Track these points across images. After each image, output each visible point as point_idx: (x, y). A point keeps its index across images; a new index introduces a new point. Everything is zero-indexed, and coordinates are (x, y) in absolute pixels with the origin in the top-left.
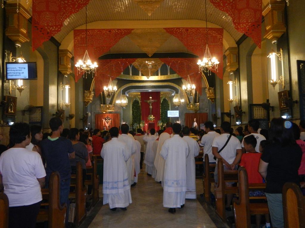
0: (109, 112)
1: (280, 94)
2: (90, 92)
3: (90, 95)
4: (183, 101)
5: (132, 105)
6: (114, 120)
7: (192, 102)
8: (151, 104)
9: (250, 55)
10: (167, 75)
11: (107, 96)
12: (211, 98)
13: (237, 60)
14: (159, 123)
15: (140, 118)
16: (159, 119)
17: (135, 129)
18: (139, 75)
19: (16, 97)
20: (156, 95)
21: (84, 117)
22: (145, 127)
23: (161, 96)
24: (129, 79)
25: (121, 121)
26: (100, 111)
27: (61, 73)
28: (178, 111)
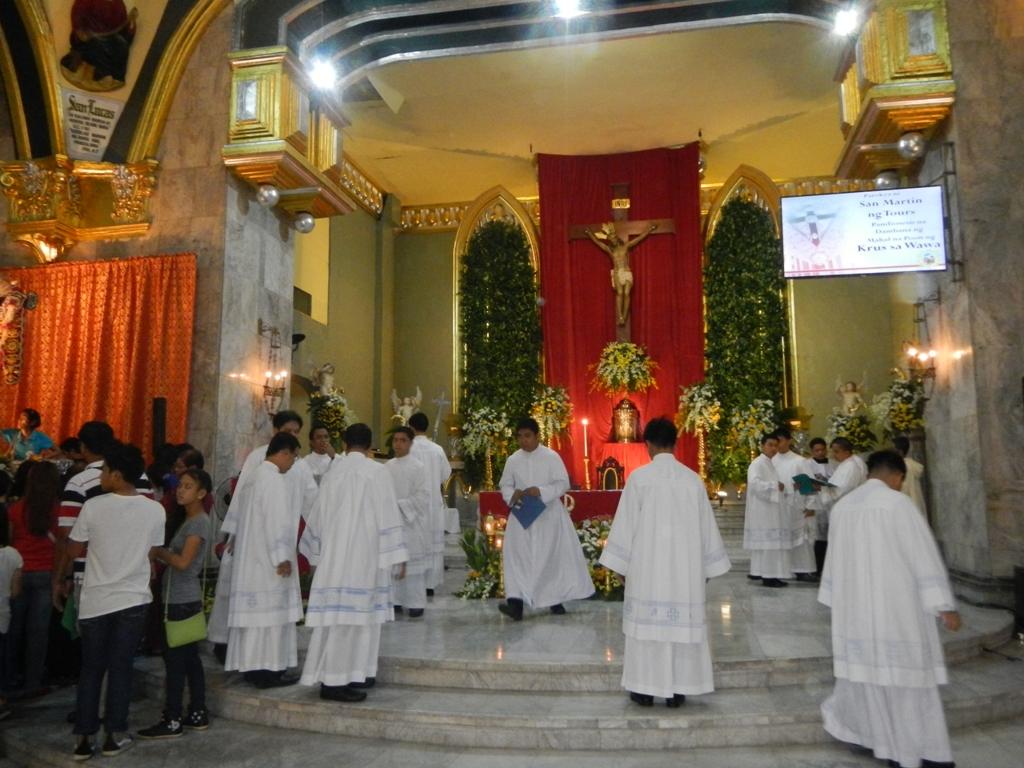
0: (101, 243)
5: (465, 260)
6: (131, 332)
8: (620, 255)
11: (67, 63)
14: (688, 410)
15: (532, 370)
16: (695, 377)
17: (480, 456)
20: (668, 173)
22: (573, 440)
23: (704, 212)
25: (203, 338)
26: (11, 246)
28: (927, 202)
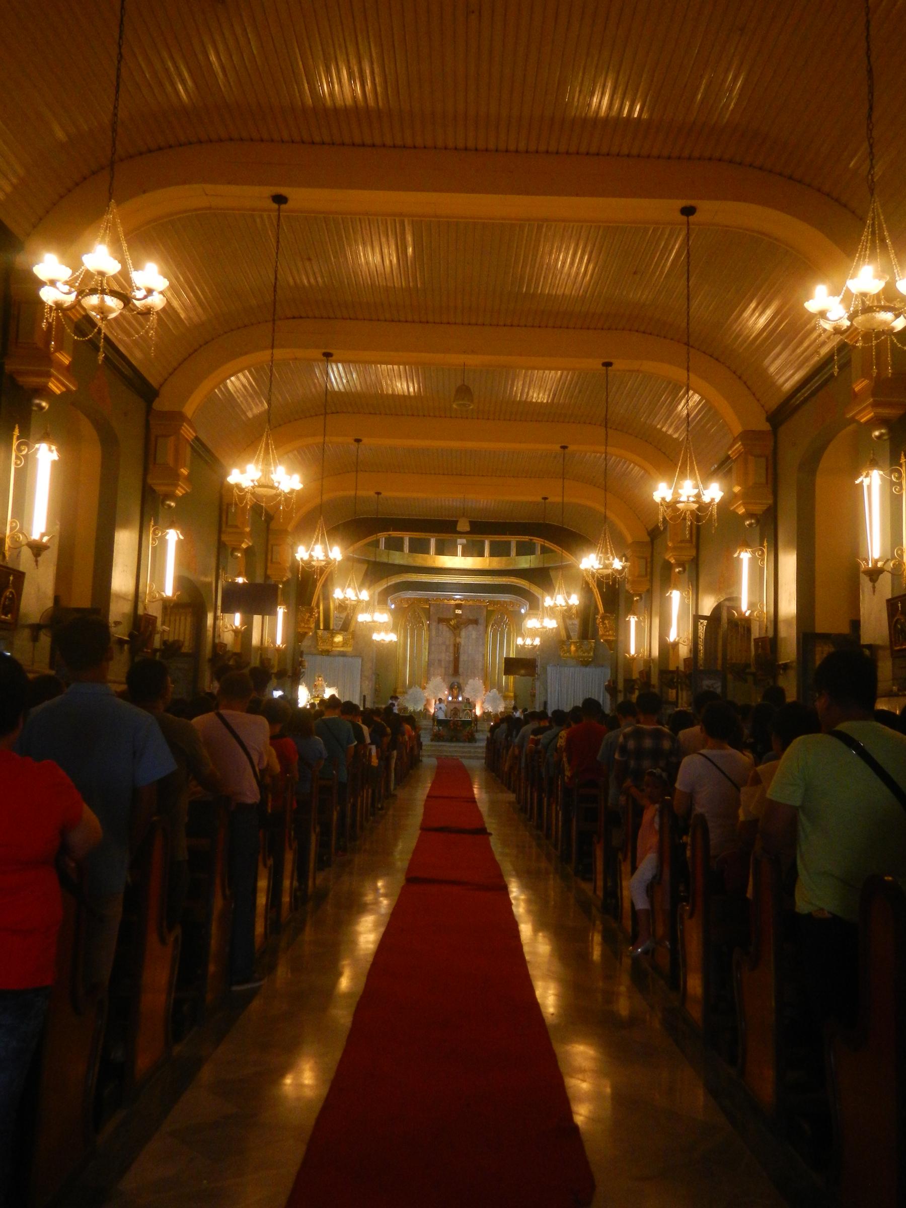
1: (685, 660)
2: (311, 611)
3: (310, 617)
4: (537, 642)
7: (575, 637)
9: (810, 464)
10: (509, 555)
12: (606, 641)
13: (649, 570)
18: (427, 551)
19: (225, 642)
21: (289, 668)
24: (401, 562)
27: (154, 491)
